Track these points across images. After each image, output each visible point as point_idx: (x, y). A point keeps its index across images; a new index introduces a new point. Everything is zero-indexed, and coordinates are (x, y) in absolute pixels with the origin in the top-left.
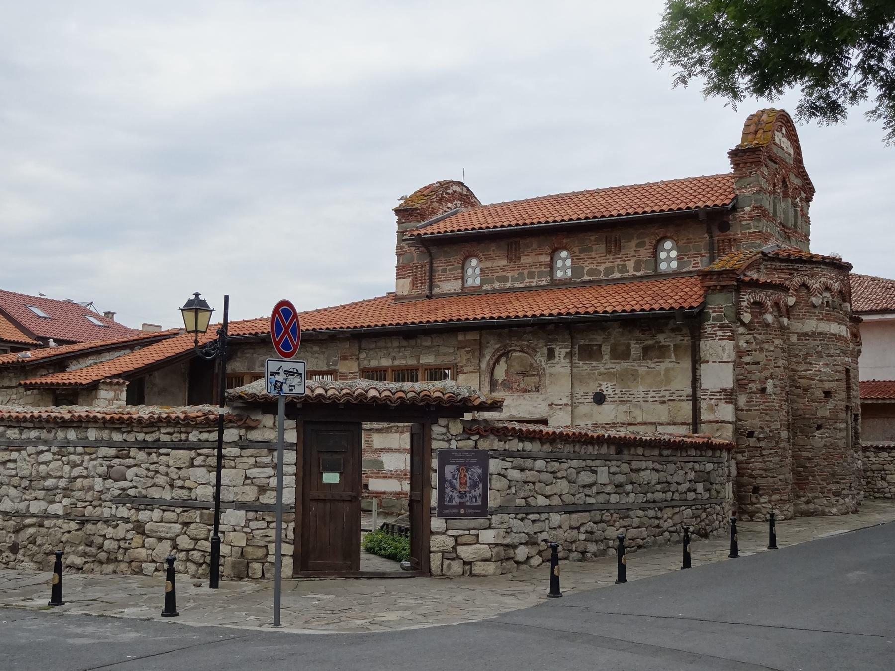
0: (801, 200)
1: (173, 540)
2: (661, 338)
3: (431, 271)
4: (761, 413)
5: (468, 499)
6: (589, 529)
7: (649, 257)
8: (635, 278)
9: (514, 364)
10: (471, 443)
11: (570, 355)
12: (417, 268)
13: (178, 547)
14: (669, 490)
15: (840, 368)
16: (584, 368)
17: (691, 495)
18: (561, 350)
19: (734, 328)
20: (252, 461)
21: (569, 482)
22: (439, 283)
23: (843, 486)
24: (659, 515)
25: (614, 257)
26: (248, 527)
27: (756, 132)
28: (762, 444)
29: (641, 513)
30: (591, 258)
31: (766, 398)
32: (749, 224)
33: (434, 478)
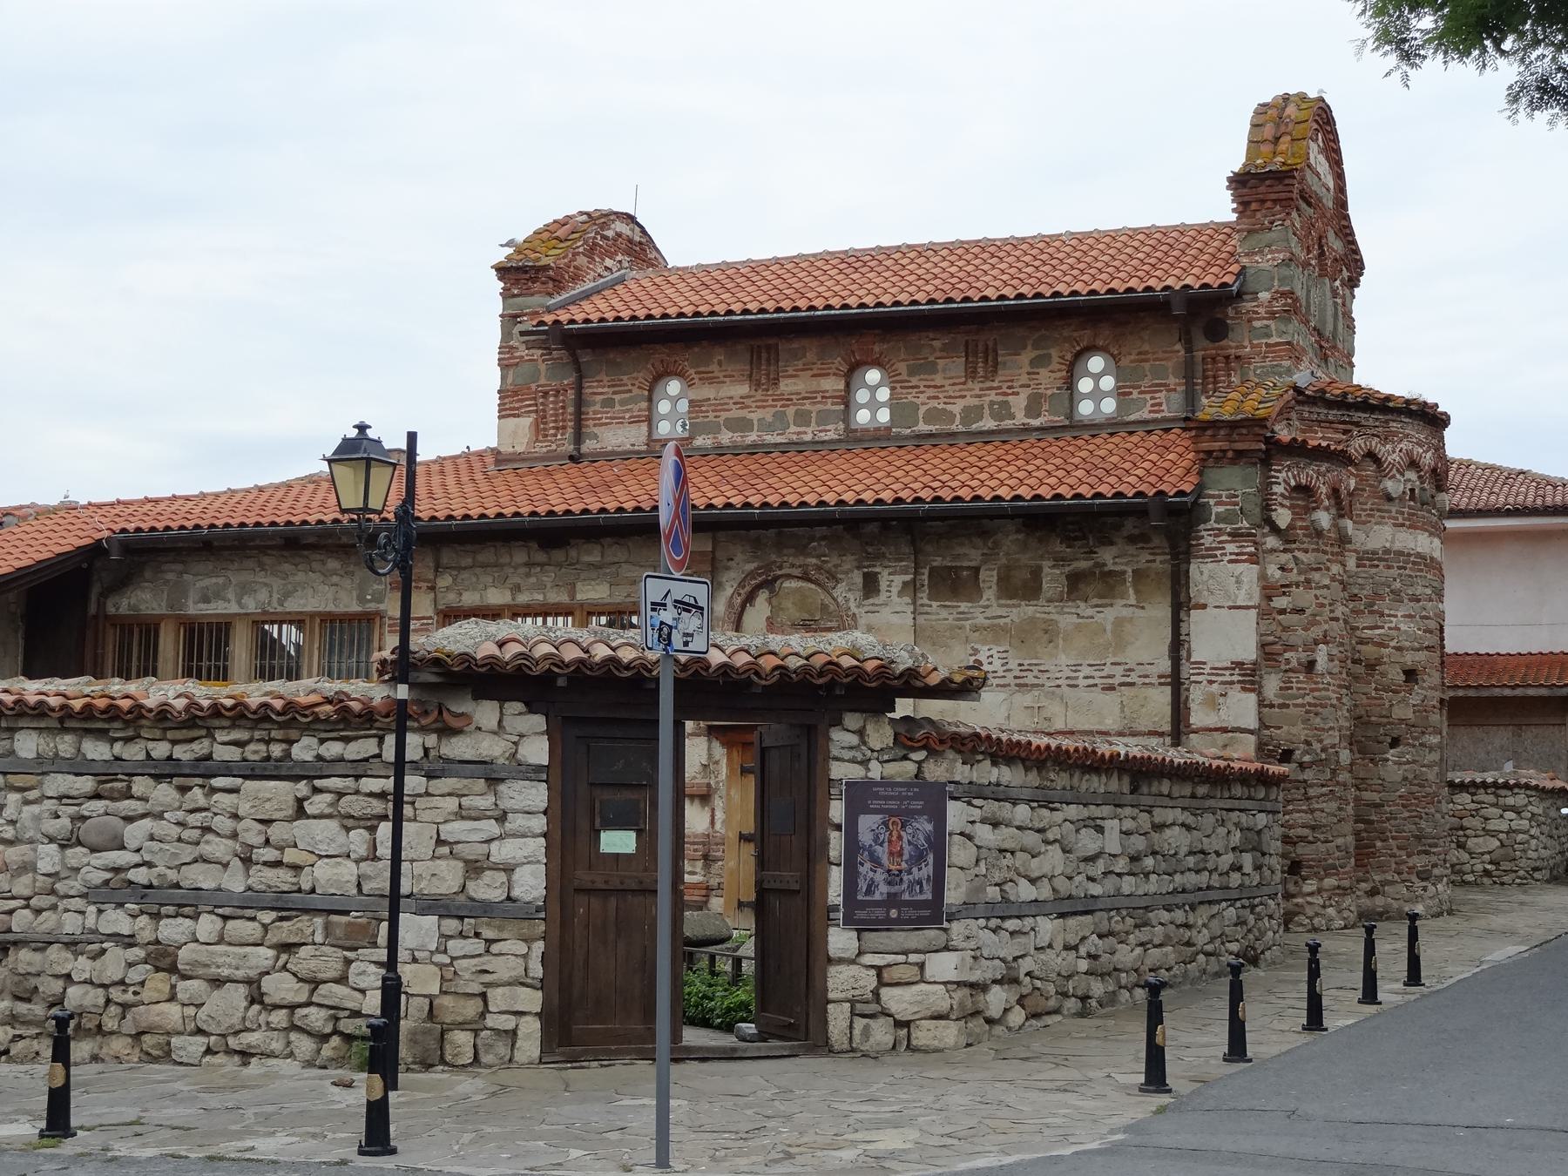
0: (1343, 284)
1: (253, 983)
2: (1107, 556)
3: (580, 403)
4: (1307, 712)
5: (905, 886)
6: (1093, 951)
7: (1058, 388)
8: (1027, 430)
9: (788, 604)
10: (909, 768)
11: (911, 588)
12: (546, 394)
13: (267, 1000)
14: (1205, 869)
16: (941, 617)
17: (1235, 879)
18: (891, 577)
19: (1258, 539)
20: (451, 804)
21: (1064, 851)
22: (596, 430)
23: (1434, 859)
24: (1191, 920)
25: (981, 385)
26: (445, 951)
27: (1277, 139)
28: (1308, 775)
29: (1165, 916)
30: (935, 387)
32: (1267, 326)
33: (836, 844)
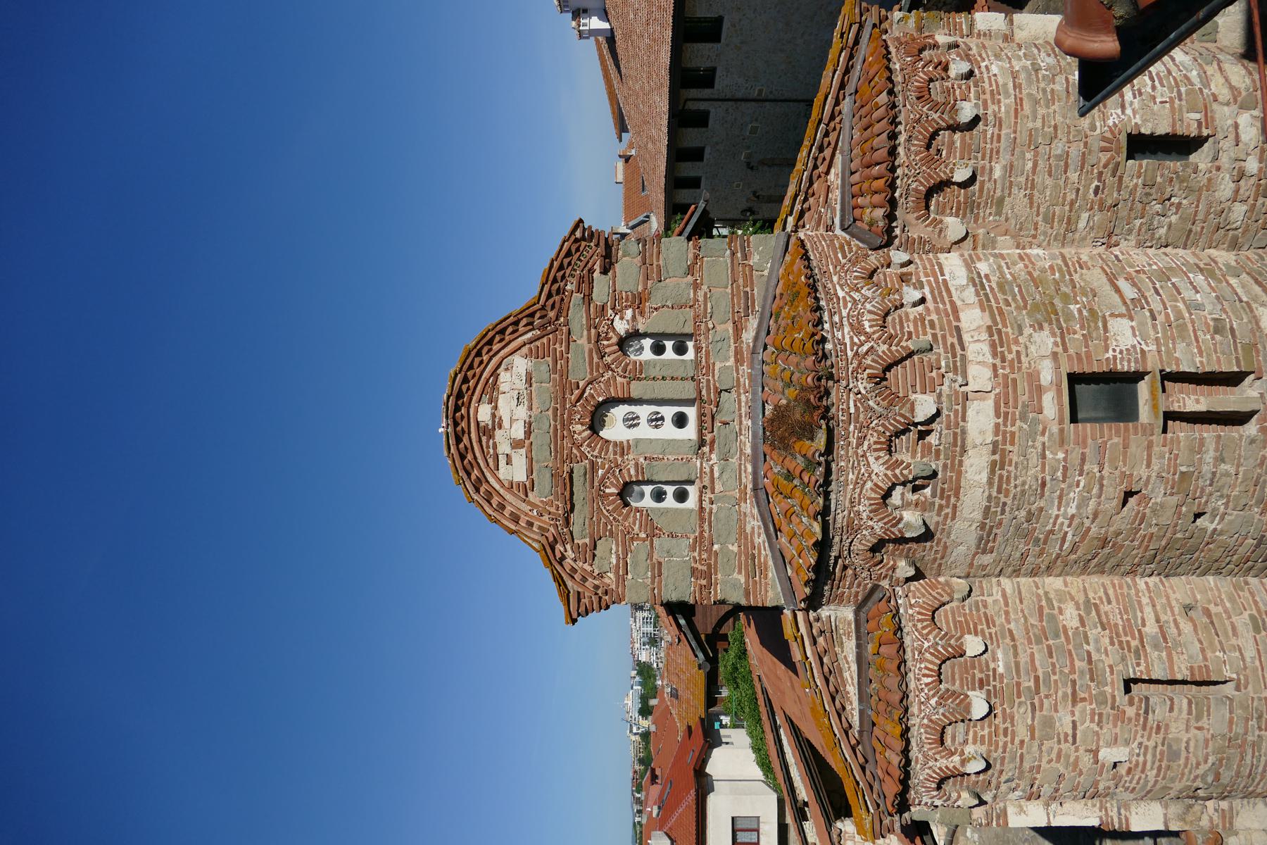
15: (1075, 457)
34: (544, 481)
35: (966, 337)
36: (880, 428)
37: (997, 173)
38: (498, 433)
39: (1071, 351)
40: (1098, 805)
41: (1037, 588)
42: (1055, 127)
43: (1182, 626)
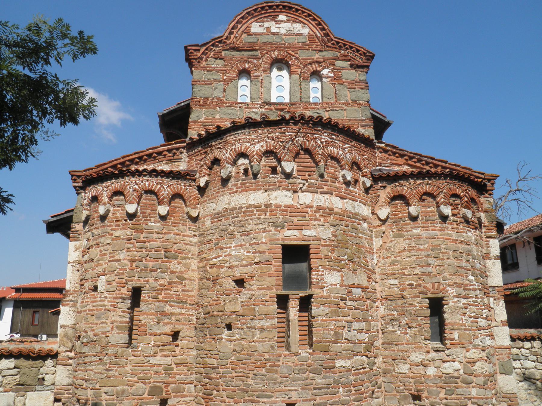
4: (87, 314)
15: (263, 247)
31: (95, 298)
34: (251, 39)
35: (327, 196)
36: (278, 146)
37: (415, 231)
38: (273, 23)
39: (322, 249)
40: (76, 289)
41: (192, 255)
42: (443, 260)
43: (168, 326)
